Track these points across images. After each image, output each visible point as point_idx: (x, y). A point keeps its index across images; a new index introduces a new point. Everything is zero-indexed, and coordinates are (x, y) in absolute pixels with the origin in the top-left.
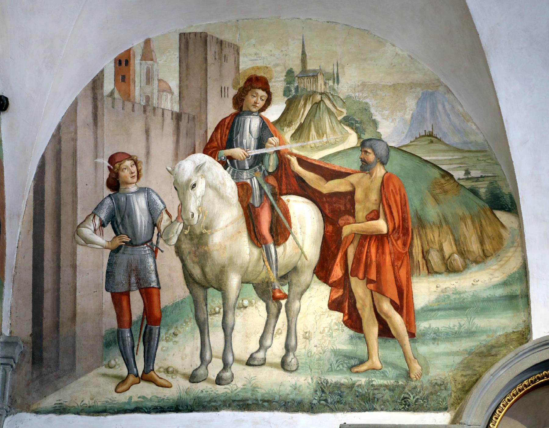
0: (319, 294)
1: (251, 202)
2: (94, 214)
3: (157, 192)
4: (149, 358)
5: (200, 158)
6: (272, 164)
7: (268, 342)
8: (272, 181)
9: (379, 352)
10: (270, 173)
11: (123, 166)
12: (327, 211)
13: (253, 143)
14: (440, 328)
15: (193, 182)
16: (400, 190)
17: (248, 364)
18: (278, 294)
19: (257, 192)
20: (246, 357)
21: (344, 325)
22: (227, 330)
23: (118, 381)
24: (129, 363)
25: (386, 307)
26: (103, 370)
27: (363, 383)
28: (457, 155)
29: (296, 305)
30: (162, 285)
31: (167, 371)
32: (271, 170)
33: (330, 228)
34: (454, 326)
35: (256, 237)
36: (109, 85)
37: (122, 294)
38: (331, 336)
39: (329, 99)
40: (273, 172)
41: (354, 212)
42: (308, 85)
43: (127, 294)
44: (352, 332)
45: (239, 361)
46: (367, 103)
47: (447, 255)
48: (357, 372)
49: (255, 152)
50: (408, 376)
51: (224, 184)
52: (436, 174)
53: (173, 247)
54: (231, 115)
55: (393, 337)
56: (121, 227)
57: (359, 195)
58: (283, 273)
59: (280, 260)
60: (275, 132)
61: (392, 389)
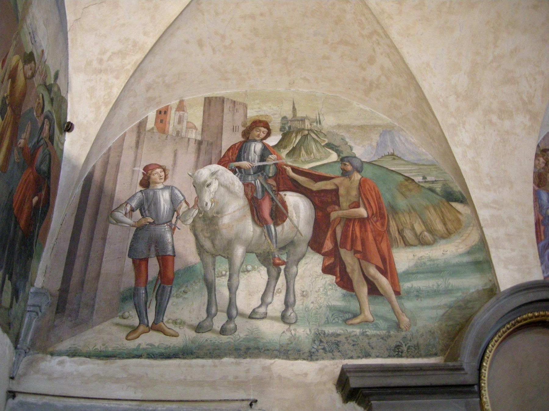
1: (255, 195)
3: (179, 188)
4: (160, 311)
5: (215, 167)
6: (272, 171)
7: (269, 299)
8: (272, 182)
9: (369, 309)
10: (270, 177)
11: (154, 172)
12: (317, 202)
13: (257, 158)
14: (421, 288)
15: (208, 182)
16: (374, 188)
17: (250, 317)
18: (277, 261)
19: (260, 190)
20: (249, 312)
21: (337, 286)
22: (232, 289)
23: (130, 330)
24: (142, 315)
25: (373, 271)
26: (117, 320)
27: (358, 334)
28: (414, 168)
29: (294, 269)
30: (176, 253)
31: (175, 322)
32: (270, 175)
33: (320, 214)
34: (433, 285)
35: (258, 218)
36: (151, 124)
37: (141, 260)
38: (326, 294)
39: (314, 133)
40: (273, 176)
41: (339, 202)
42: (298, 125)
43: (146, 260)
44: (344, 291)
45: (242, 315)
46: (342, 136)
47: (418, 233)
48: (351, 324)
49: (257, 164)
50: (398, 326)
51: (233, 184)
52: (401, 179)
53: (189, 226)
54: (241, 142)
55: (381, 295)
56: (147, 212)
57: (342, 191)
58: (282, 245)
59: (278, 236)
60: (274, 152)
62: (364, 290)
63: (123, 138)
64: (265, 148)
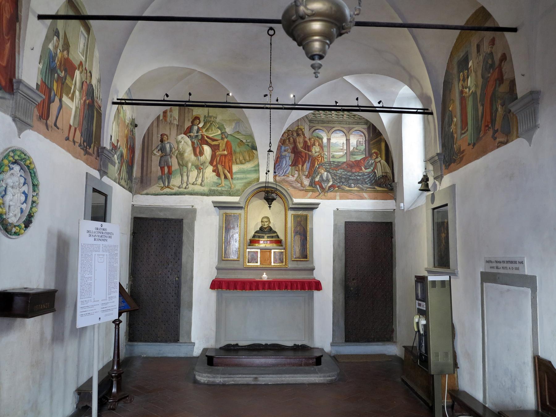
0: (210, 169)
2: (157, 148)
4: (169, 183)
5: (183, 135)
6: (200, 137)
9: (224, 182)
24: (164, 183)
25: (226, 172)
35: (195, 154)
36: (161, 118)
42: (209, 119)
50: (231, 188)
52: (239, 141)
57: (220, 145)
61: (227, 191)
62: (223, 177)
63: (153, 123)
64: (198, 128)
